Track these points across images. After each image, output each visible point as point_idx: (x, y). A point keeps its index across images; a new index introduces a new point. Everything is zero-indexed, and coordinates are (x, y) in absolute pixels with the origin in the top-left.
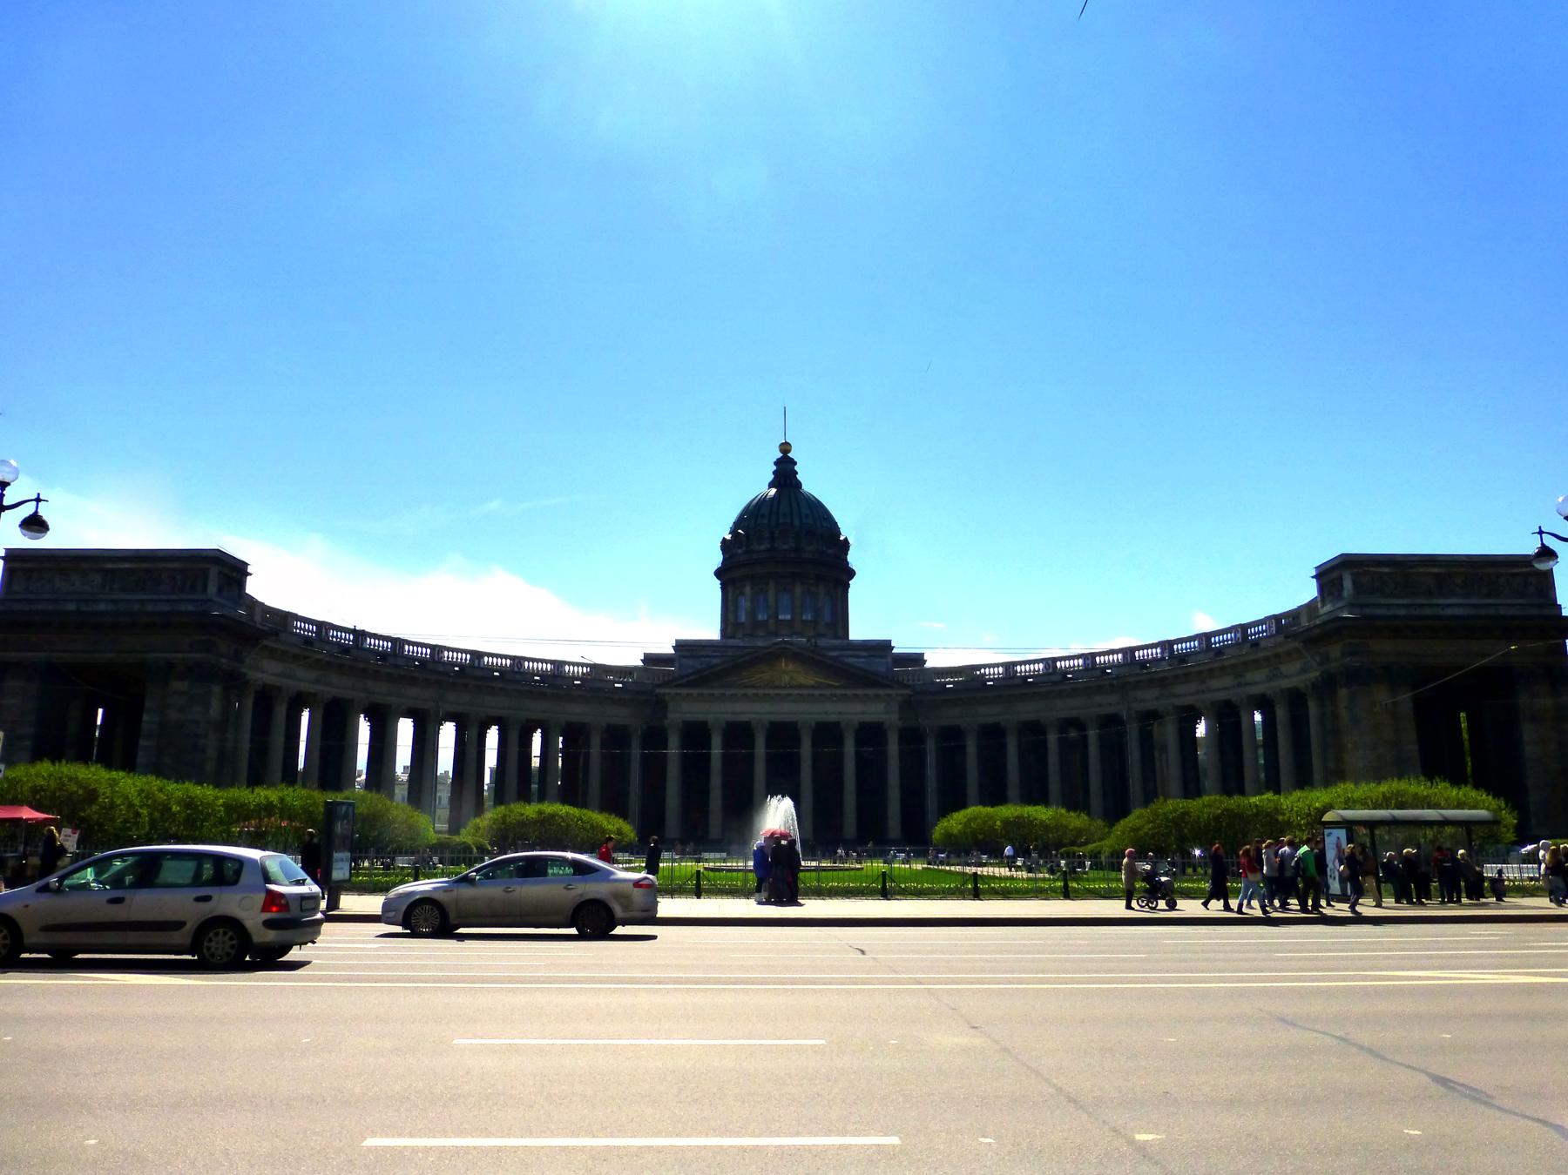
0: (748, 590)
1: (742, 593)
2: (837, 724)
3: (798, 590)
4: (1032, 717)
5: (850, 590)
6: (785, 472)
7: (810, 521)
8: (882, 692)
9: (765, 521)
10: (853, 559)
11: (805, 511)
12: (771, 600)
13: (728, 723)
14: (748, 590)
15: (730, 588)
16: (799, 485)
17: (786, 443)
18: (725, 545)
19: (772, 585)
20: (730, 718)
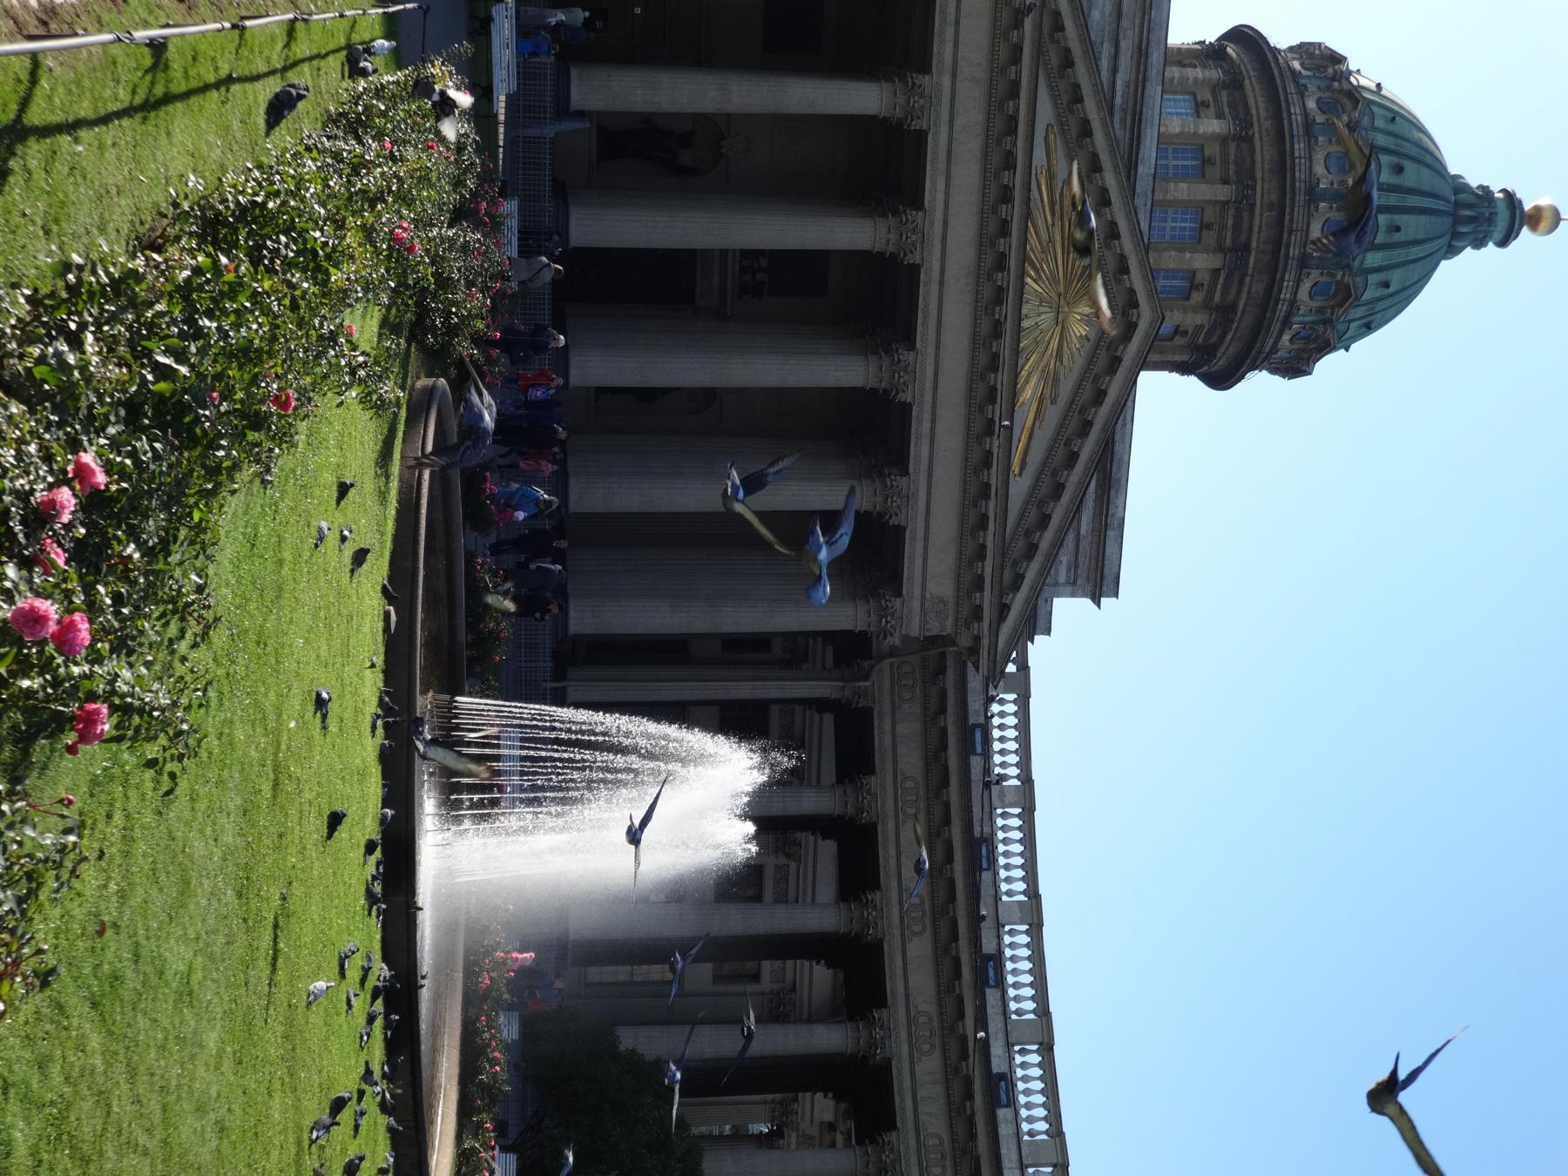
0: (1212, 126)
1: (1199, 107)
2: (899, 460)
3: (1202, 262)
4: (895, 986)
5: (1175, 375)
6: (1490, 218)
7: (1367, 295)
8: (987, 599)
9: (1386, 177)
10: (1259, 384)
11: (1396, 278)
12: (1182, 190)
13: (921, 136)
14: (1212, 126)
15: (1215, 74)
16: (1452, 251)
17: (1557, 219)
18: (1324, 63)
19: (1223, 192)
20: (937, 145)
